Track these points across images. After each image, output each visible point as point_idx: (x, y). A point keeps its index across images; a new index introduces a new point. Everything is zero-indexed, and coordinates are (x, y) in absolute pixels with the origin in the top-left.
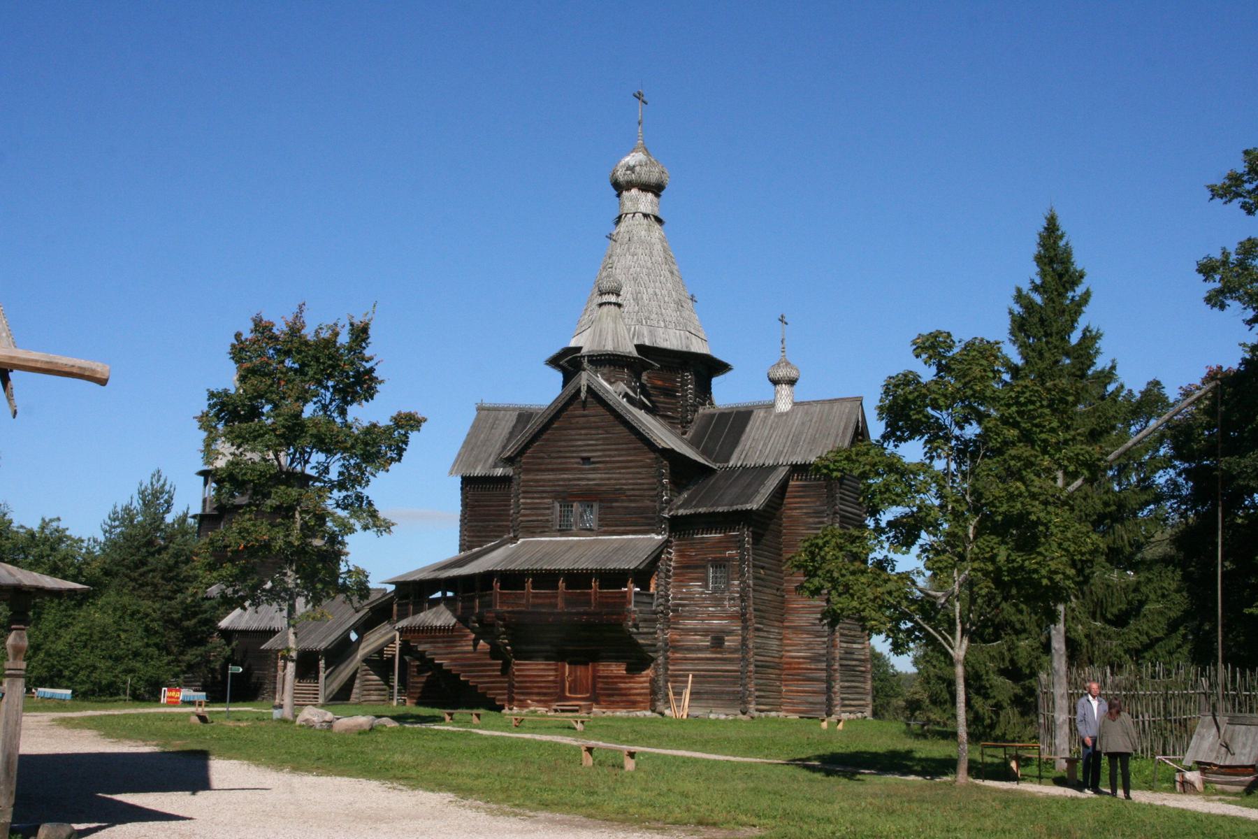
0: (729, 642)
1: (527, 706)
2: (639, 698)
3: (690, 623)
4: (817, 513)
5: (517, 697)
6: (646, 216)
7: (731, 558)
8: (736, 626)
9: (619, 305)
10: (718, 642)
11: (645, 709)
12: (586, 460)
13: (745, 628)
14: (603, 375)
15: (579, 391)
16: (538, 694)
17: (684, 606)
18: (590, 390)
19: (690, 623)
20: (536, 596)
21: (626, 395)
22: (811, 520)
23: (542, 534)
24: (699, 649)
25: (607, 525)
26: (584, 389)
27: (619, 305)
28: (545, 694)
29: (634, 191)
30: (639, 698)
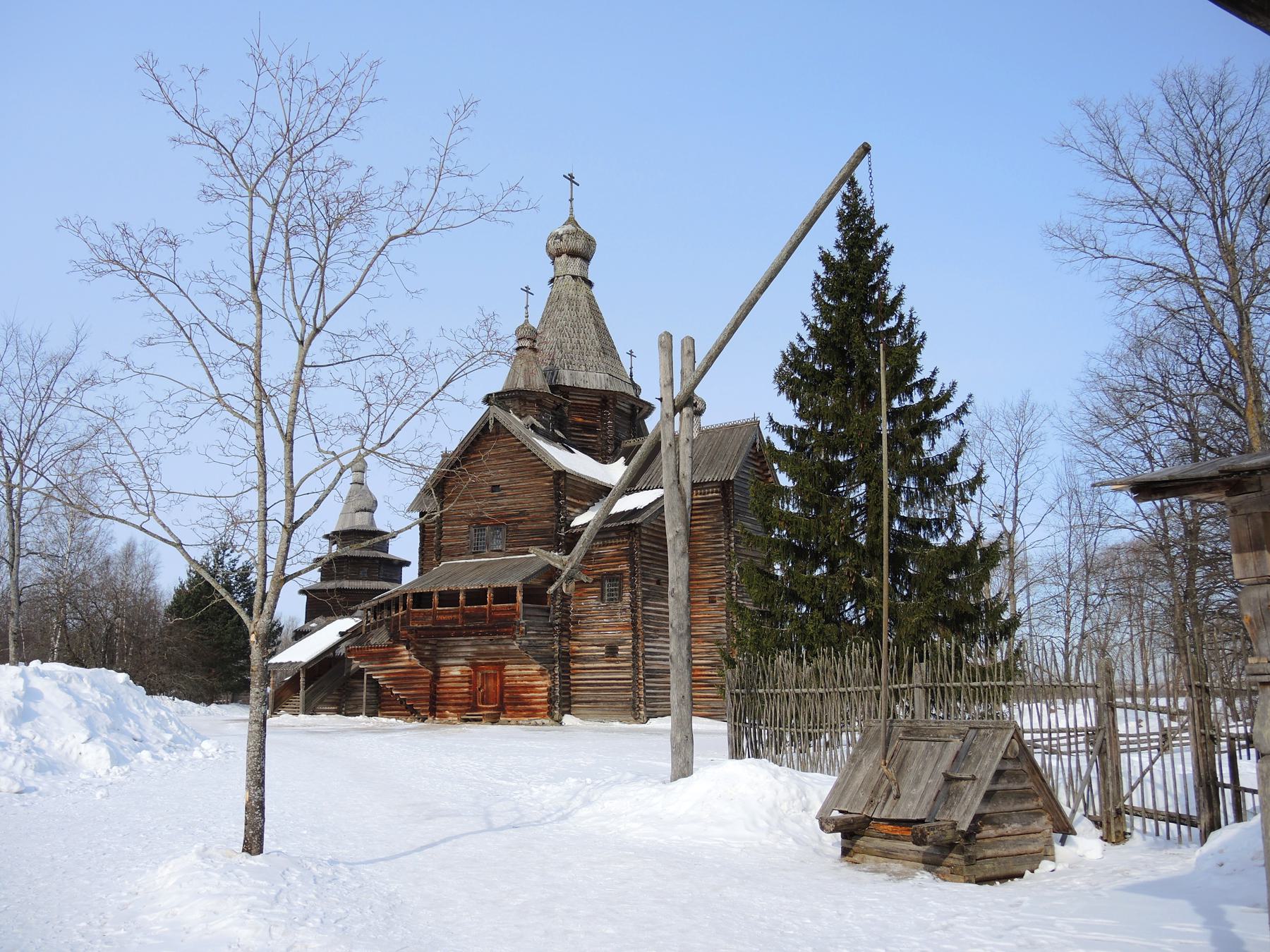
0: (624, 650)
1: (446, 717)
2: (538, 707)
3: (588, 635)
4: (716, 529)
5: (439, 708)
6: (574, 277)
7: (621, 573)
8: (628, 635)
9: (535, 350)
10: (612, 651)
11: (544, 716)
12: (495, 488)
13: (635, 637)
14: (514, 410)
15: (488, 424)
16: (456, 705)
17: (581, 618)
18: (496, 421)
19: (588, 635)
20: (441, 613)
21: (533, 427)
22: (710, 536)
23: (460, 556)
24: (595, 659)
25: (514, 546)
26: (491, 423)
27: (535, 350)
28: (460, 705)
29: (564, 257)
30: (538, 707)
